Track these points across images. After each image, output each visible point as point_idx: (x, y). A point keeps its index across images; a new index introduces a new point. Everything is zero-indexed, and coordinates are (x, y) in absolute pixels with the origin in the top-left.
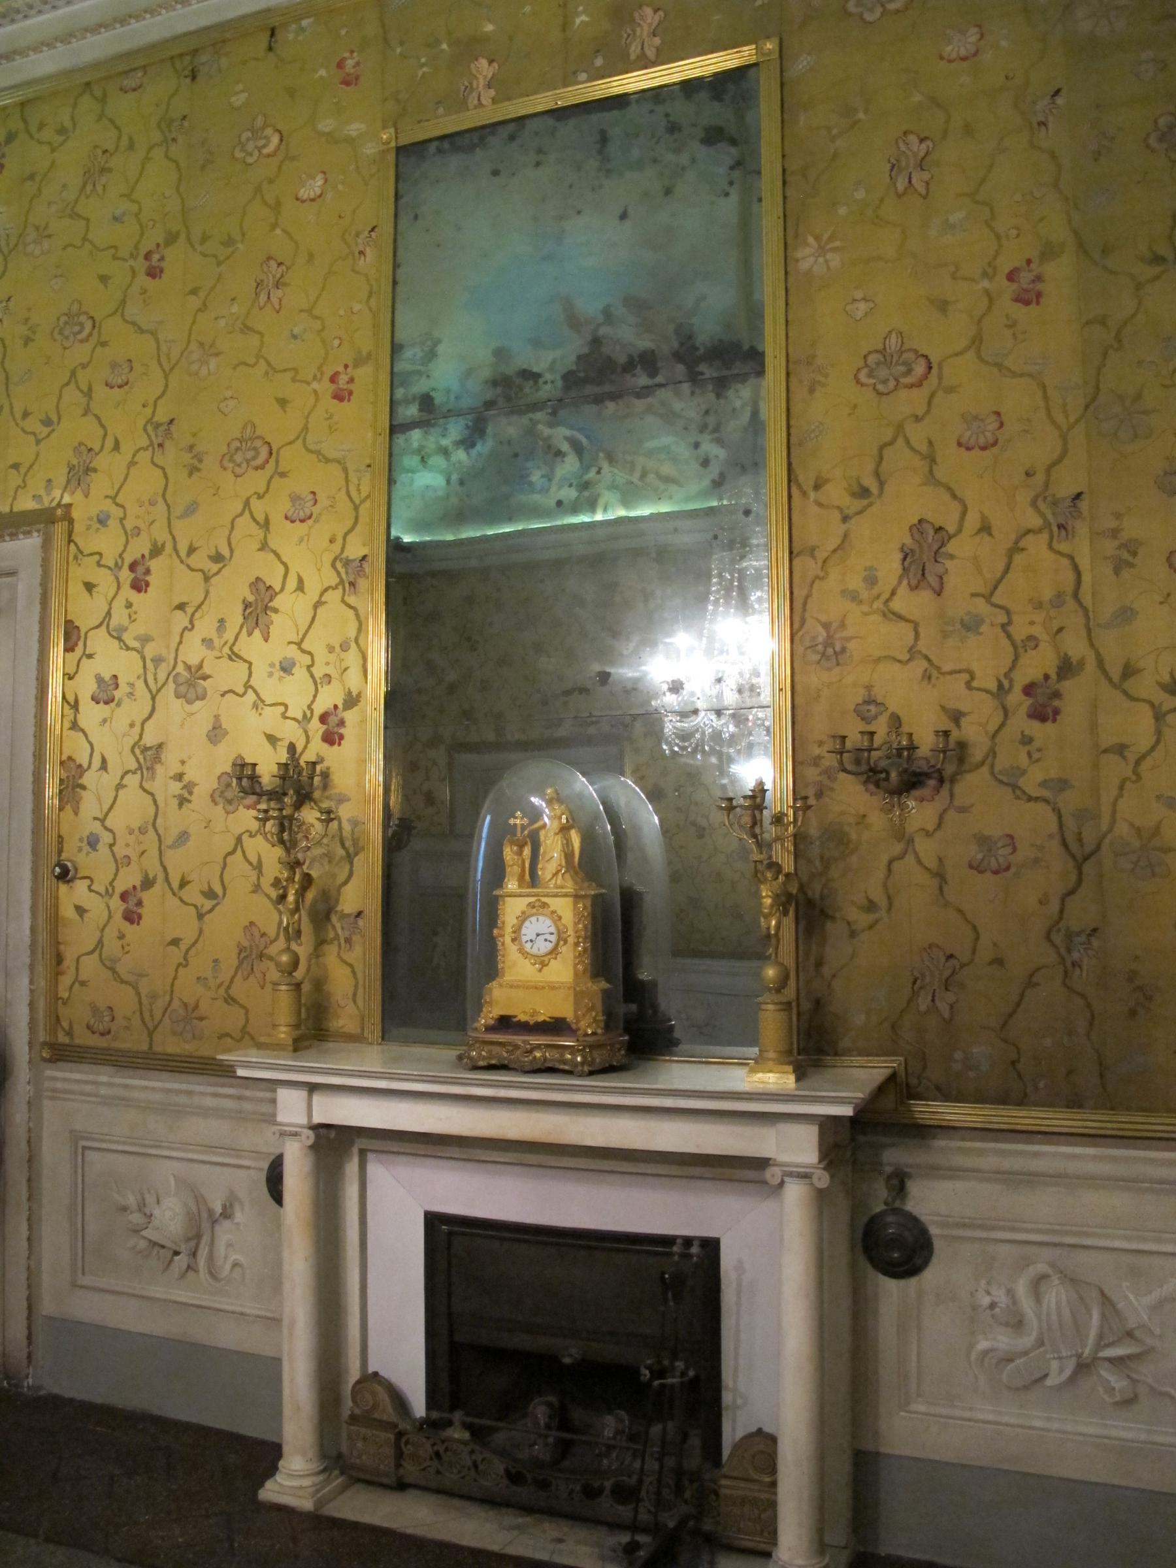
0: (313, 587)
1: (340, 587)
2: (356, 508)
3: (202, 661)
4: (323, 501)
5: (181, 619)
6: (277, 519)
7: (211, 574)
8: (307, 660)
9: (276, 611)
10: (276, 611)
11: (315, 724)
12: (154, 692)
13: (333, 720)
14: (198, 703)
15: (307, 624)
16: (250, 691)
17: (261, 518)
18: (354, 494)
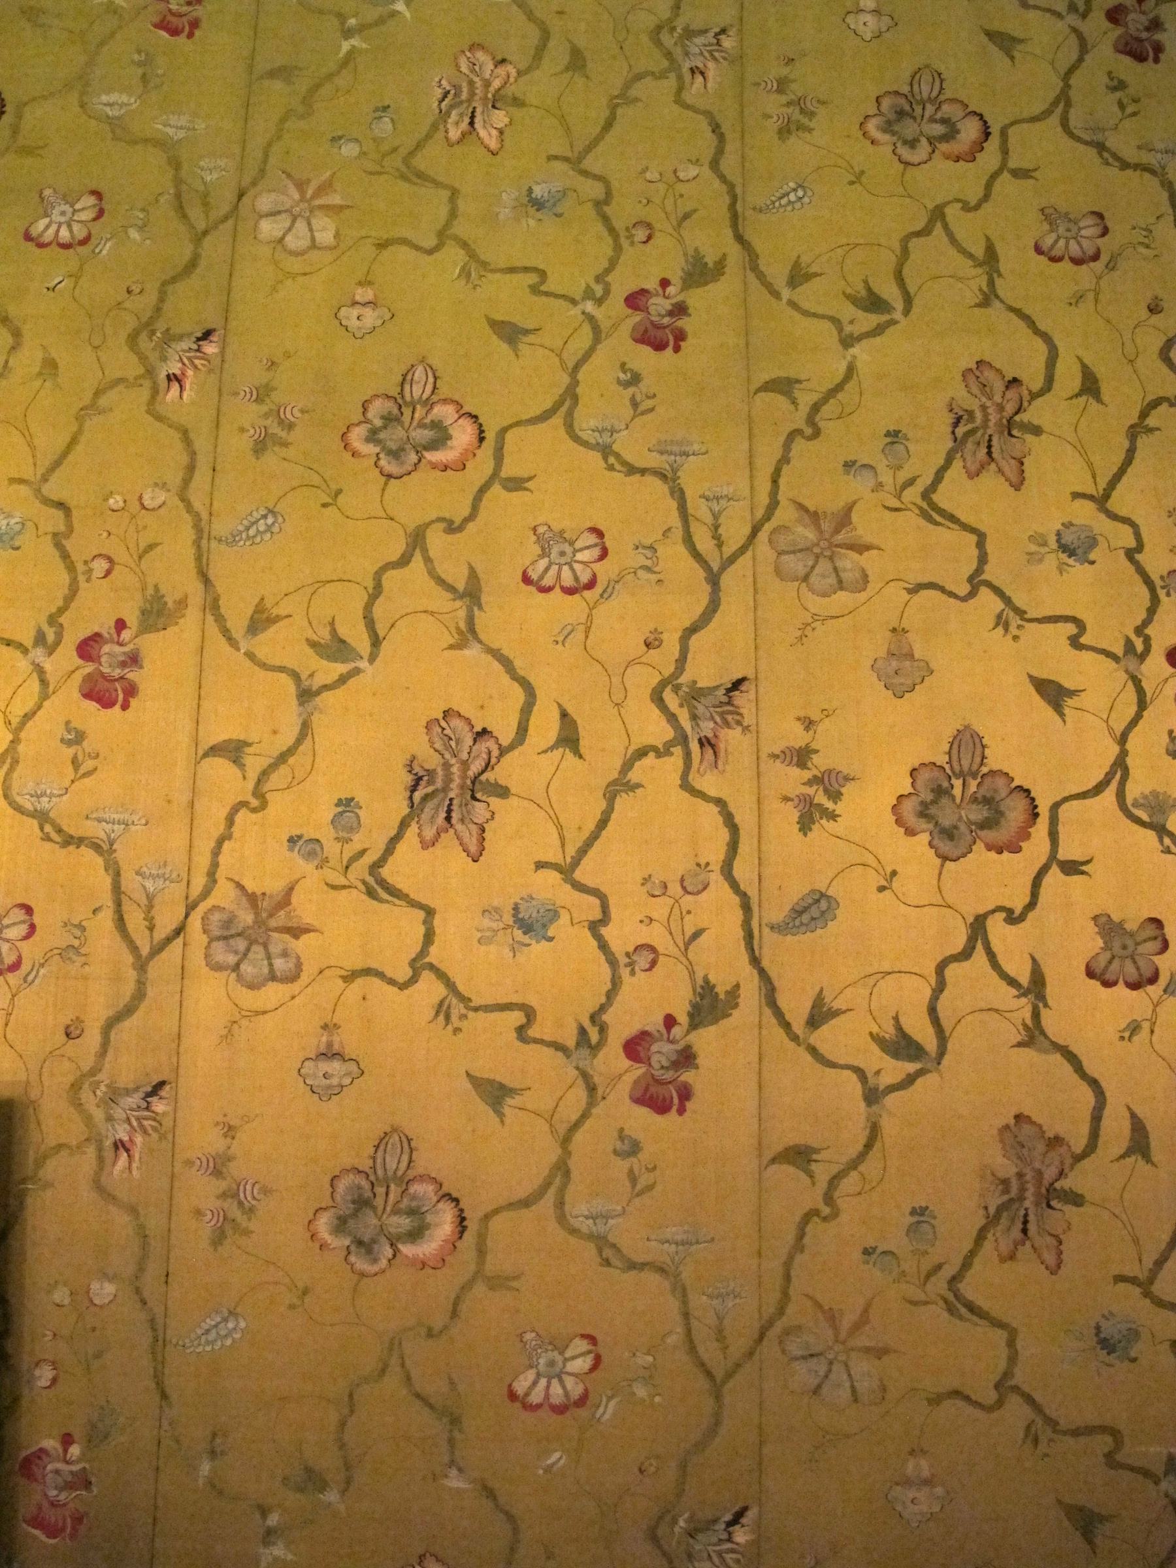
0: (605, 748)
1: (678, 751)
2: (714, 580)
3: (291, 889)
4: (623, 556)
5: (227, 781)
6: (501, 581)
7: (317, 682)
8: (590, 908)
9: (503, 792)
10: (503, 792)
11: (612, 1060)
12: (145, 951)
13: (661, 1053)
14: (273, 993)
15: (591, 826)
16: (427, 975)
17: (458, 578)
18: (704, 543)
